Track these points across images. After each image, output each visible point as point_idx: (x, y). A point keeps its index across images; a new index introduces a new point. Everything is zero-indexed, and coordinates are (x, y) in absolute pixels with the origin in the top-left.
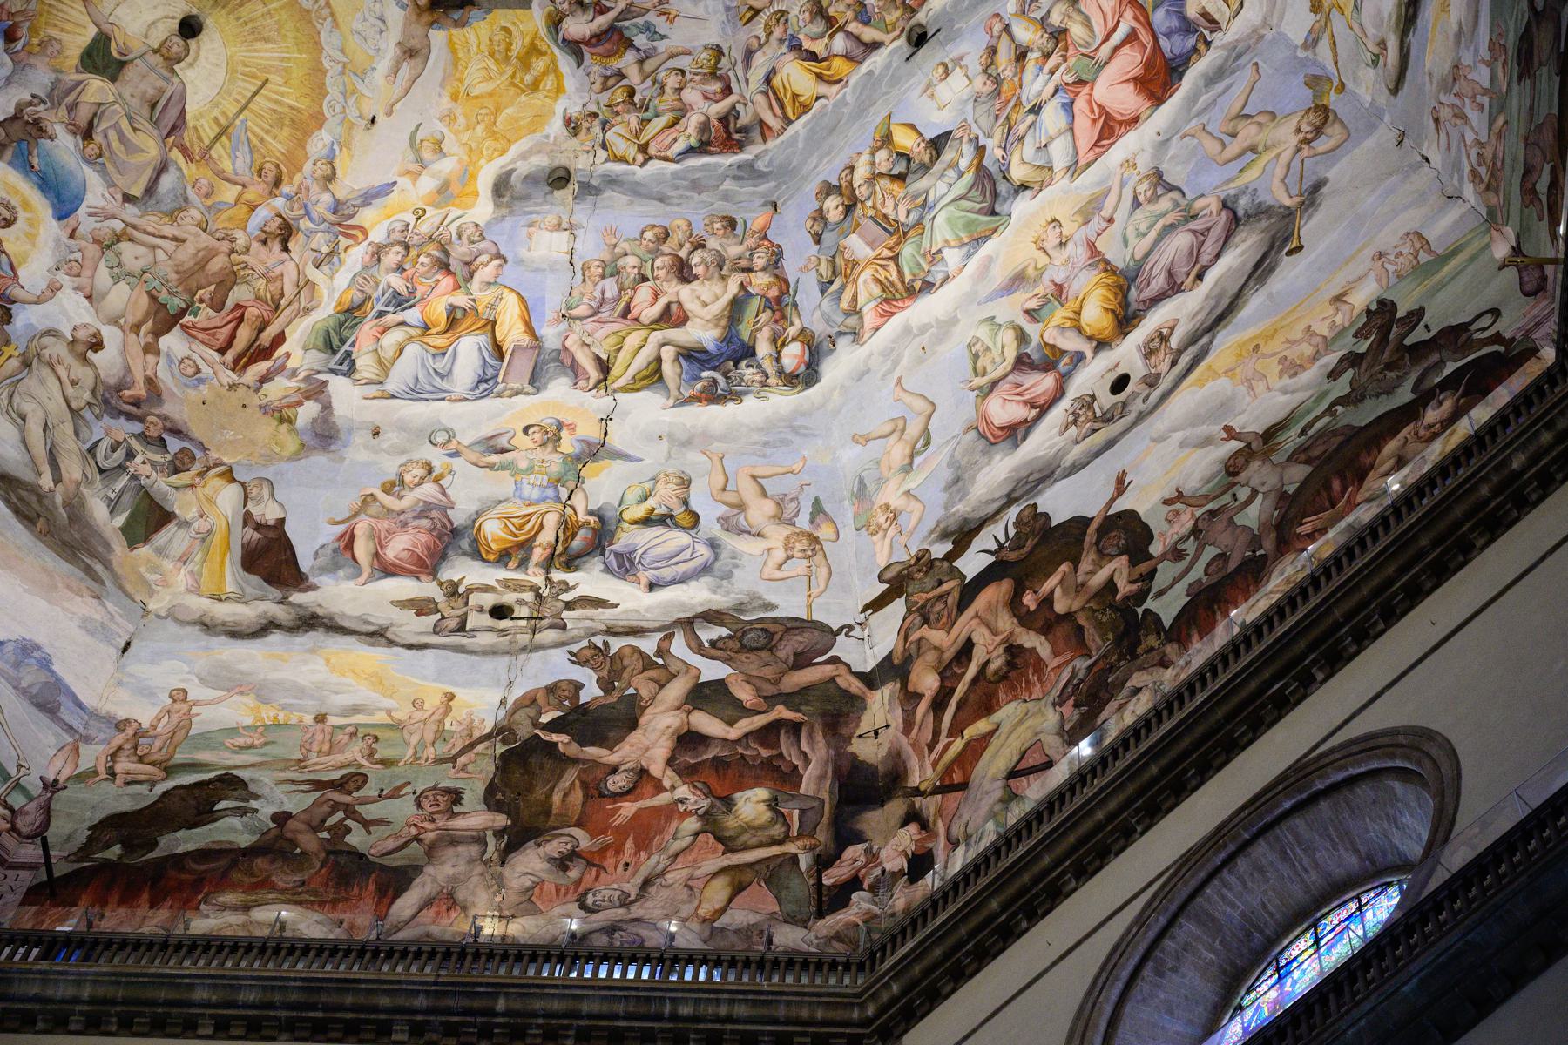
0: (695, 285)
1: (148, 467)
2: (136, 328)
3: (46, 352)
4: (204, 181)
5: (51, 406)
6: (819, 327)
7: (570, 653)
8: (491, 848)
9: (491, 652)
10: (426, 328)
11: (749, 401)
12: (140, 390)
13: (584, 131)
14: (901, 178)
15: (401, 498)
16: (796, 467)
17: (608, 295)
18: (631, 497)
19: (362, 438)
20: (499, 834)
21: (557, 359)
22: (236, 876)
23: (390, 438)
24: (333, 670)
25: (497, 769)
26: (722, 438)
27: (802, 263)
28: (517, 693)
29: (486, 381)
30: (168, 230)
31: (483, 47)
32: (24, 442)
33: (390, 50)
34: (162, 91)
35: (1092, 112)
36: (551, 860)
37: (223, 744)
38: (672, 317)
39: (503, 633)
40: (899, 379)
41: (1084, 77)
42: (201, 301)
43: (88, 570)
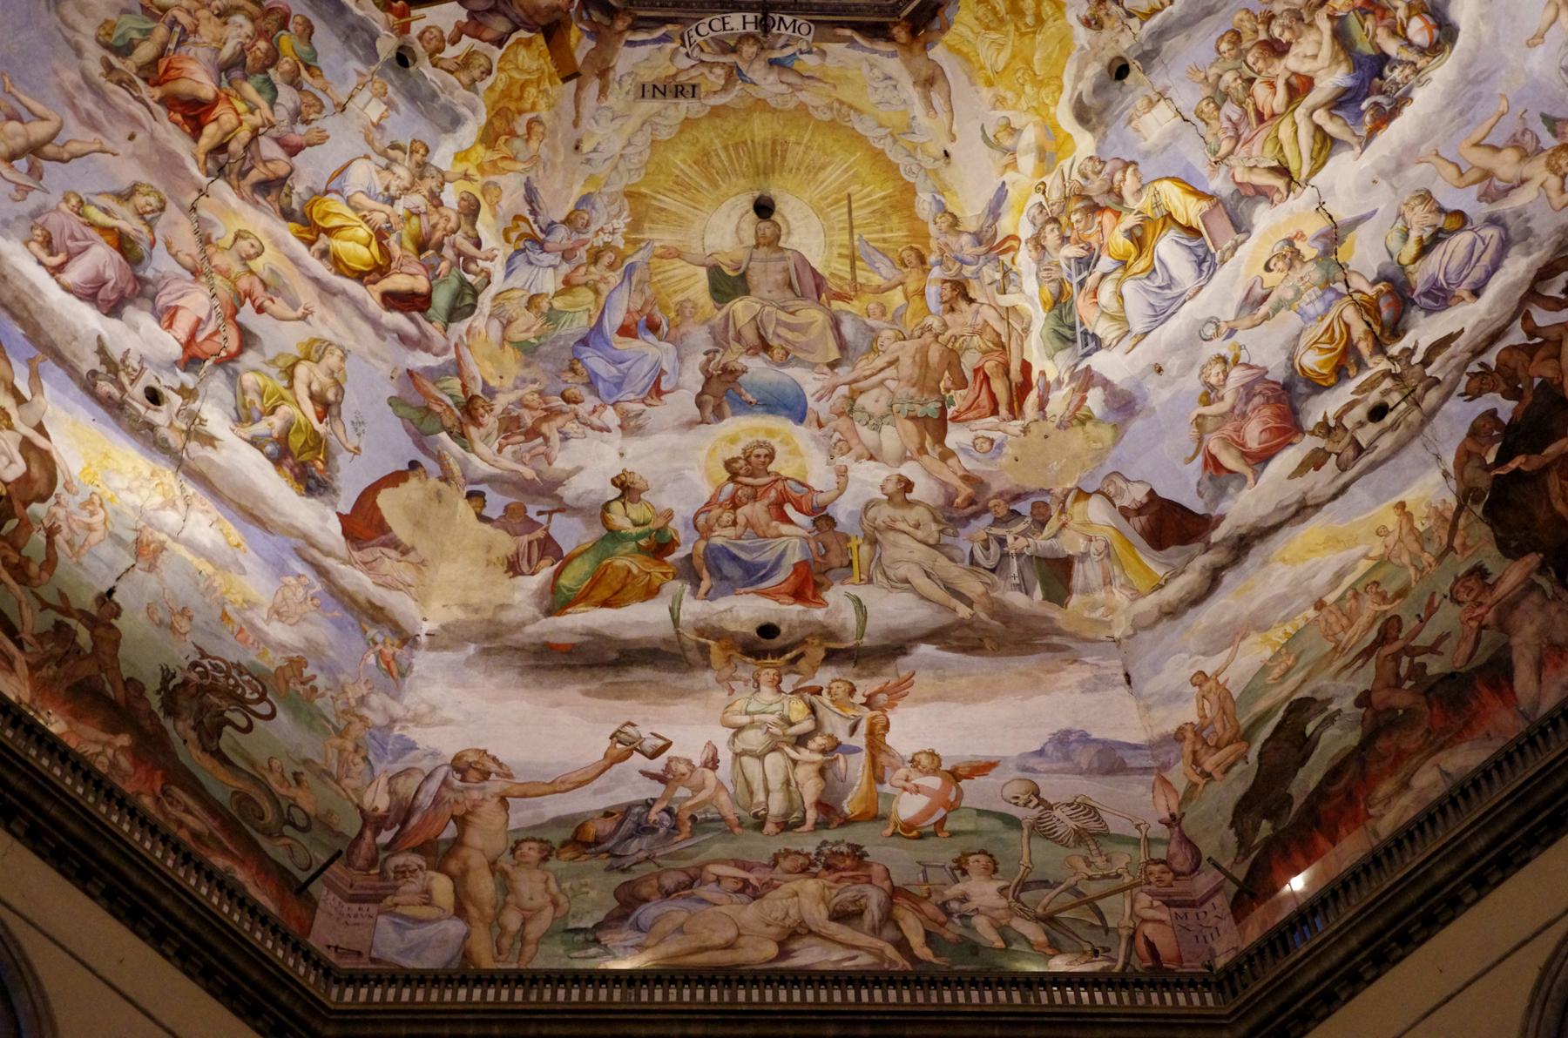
0: (1294, 50)
1: (1022, 541)
2: (922, 450)
3: (879, 522)
4: (872, 306)
5: (917, 556)
7: (1461, 395)
9: (1399, 448)
10: (1123, 264)
11: (1419, 95)
12: (965, 491)
13: (1105, 19)
15: (1222, 399)
16: (1503, 106)
17: (1235, 117)
18: (1395, 244)
19: (1152, 383)
20: (1542, 569)
21: (1242, 197)
22: (1374, 769)
23: (1173, 364)
26: (1423, 139)
28: (1450, 459)
29: (1204, 260)
30: (880, 362)
31: (977, 29)
32: (923, 597)
33: (911, 93)
34: (786, 270)
37: (1266, 686)
38: (1298, 88)
39: (1394, 426)
42: (948, 390)
43: (1052, 648)
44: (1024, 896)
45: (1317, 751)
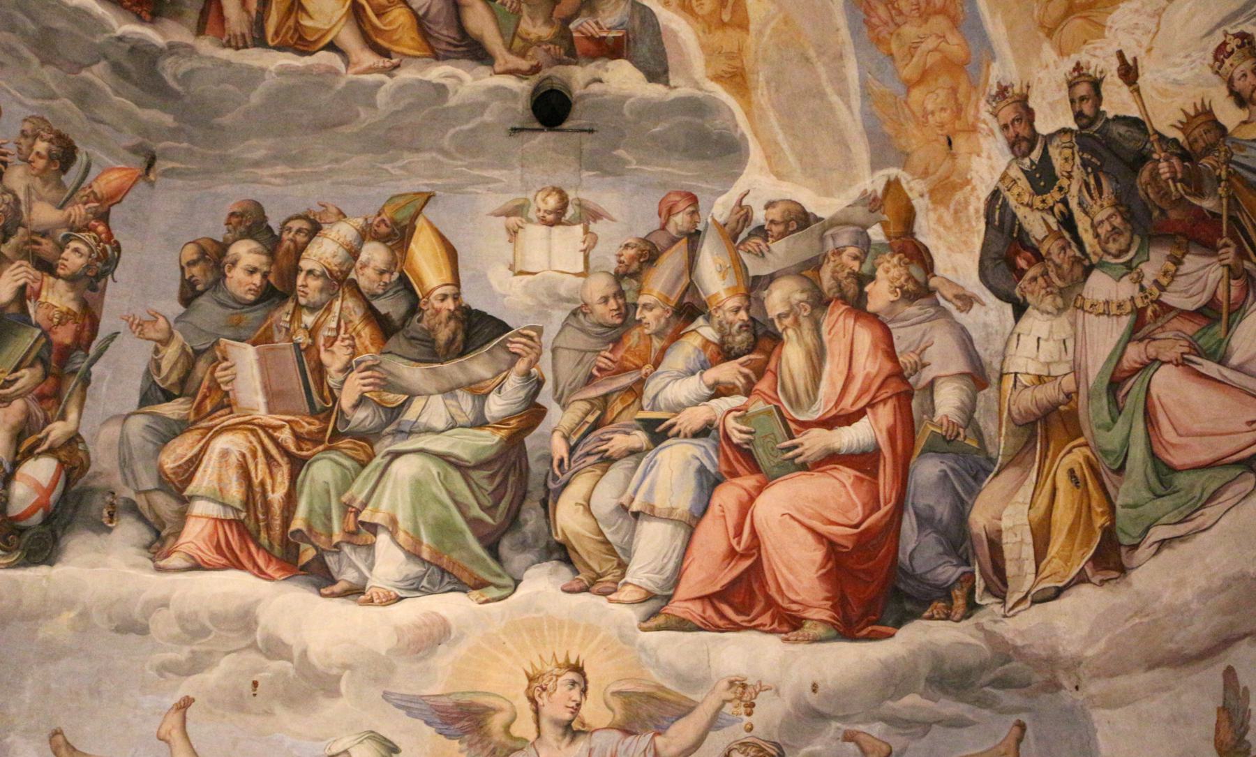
6: (103, 459)
14: (384, 327)
27: (141, 314)
35: (739, 534)
40: (185, 705)
41: (760, 453)
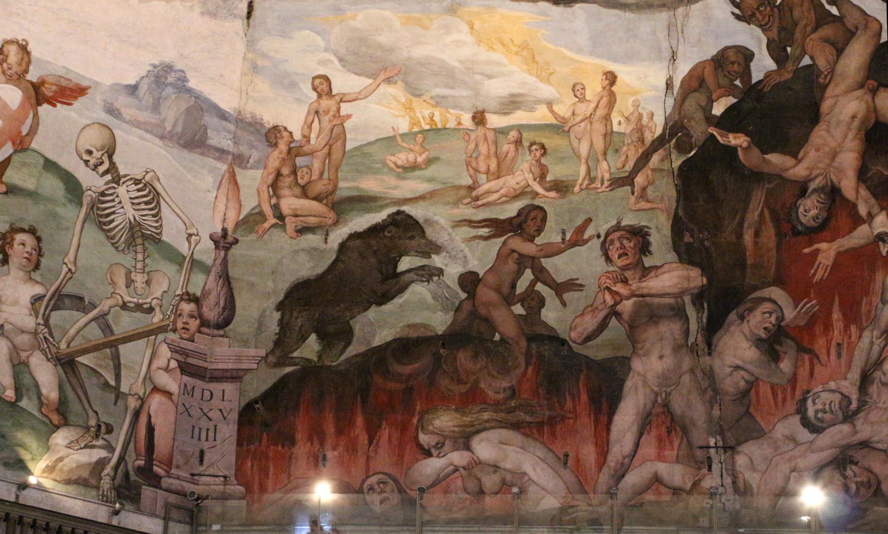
8: (693, 326)
20: (699, 298)
24: (479, 42)
25: (678, 192)
28: (683, 69)
36: (758, 342)
37: (384, 163)
44: (56, 317)
45: (398, 301)
